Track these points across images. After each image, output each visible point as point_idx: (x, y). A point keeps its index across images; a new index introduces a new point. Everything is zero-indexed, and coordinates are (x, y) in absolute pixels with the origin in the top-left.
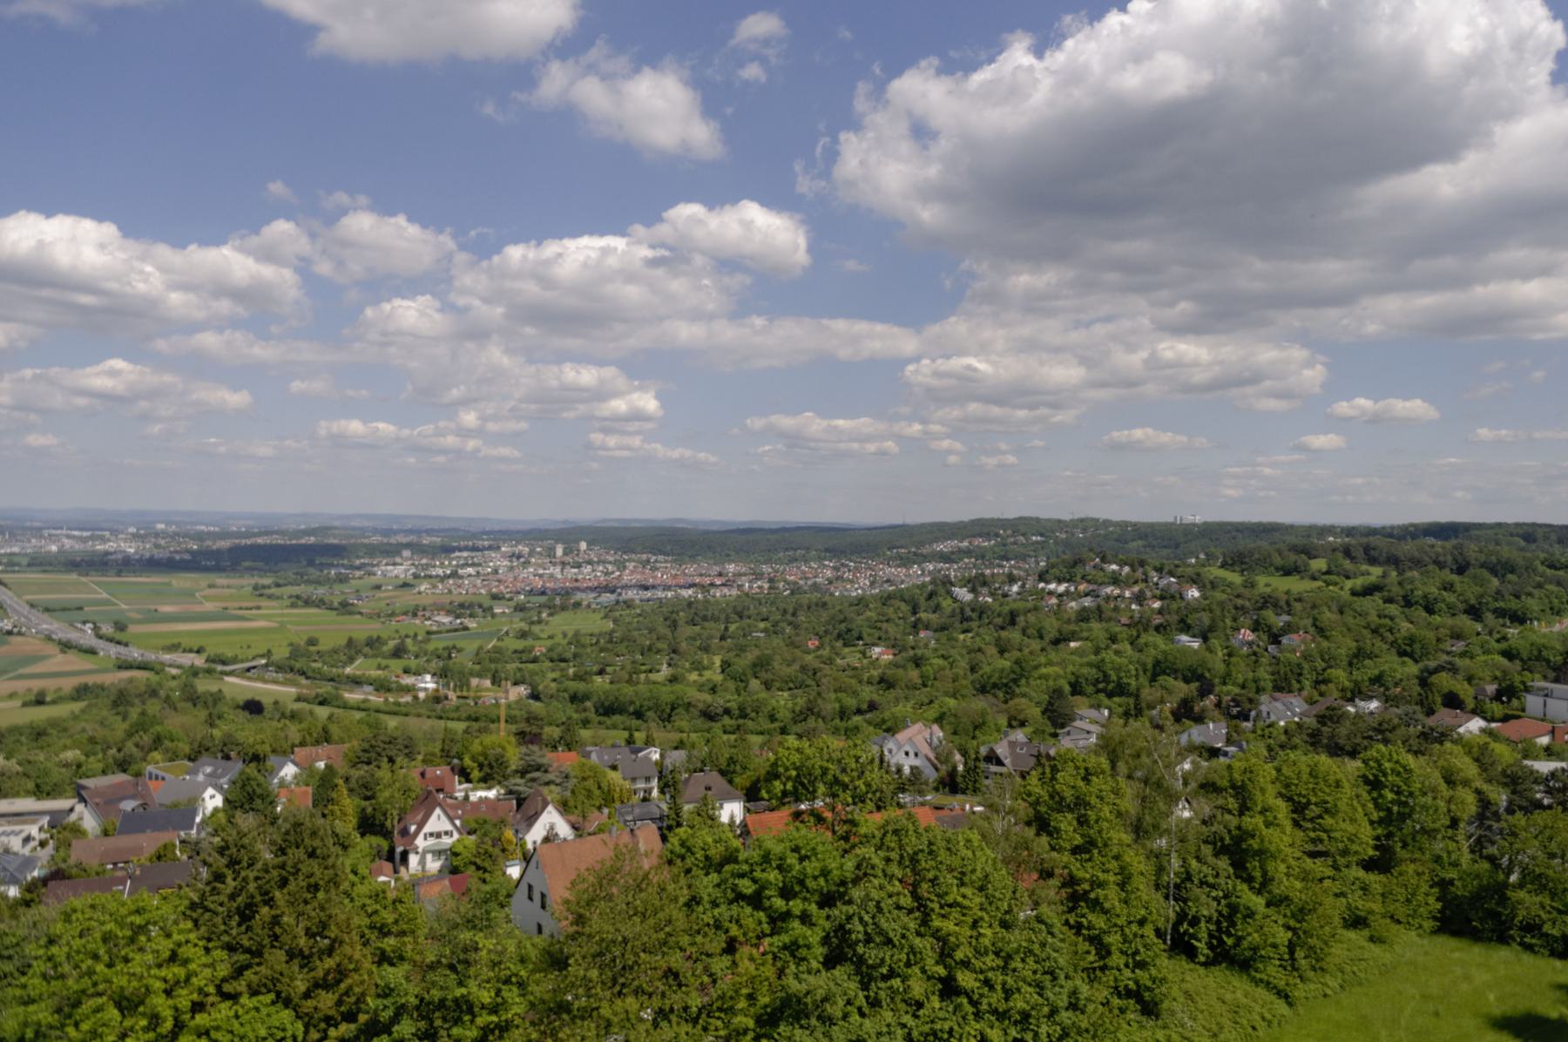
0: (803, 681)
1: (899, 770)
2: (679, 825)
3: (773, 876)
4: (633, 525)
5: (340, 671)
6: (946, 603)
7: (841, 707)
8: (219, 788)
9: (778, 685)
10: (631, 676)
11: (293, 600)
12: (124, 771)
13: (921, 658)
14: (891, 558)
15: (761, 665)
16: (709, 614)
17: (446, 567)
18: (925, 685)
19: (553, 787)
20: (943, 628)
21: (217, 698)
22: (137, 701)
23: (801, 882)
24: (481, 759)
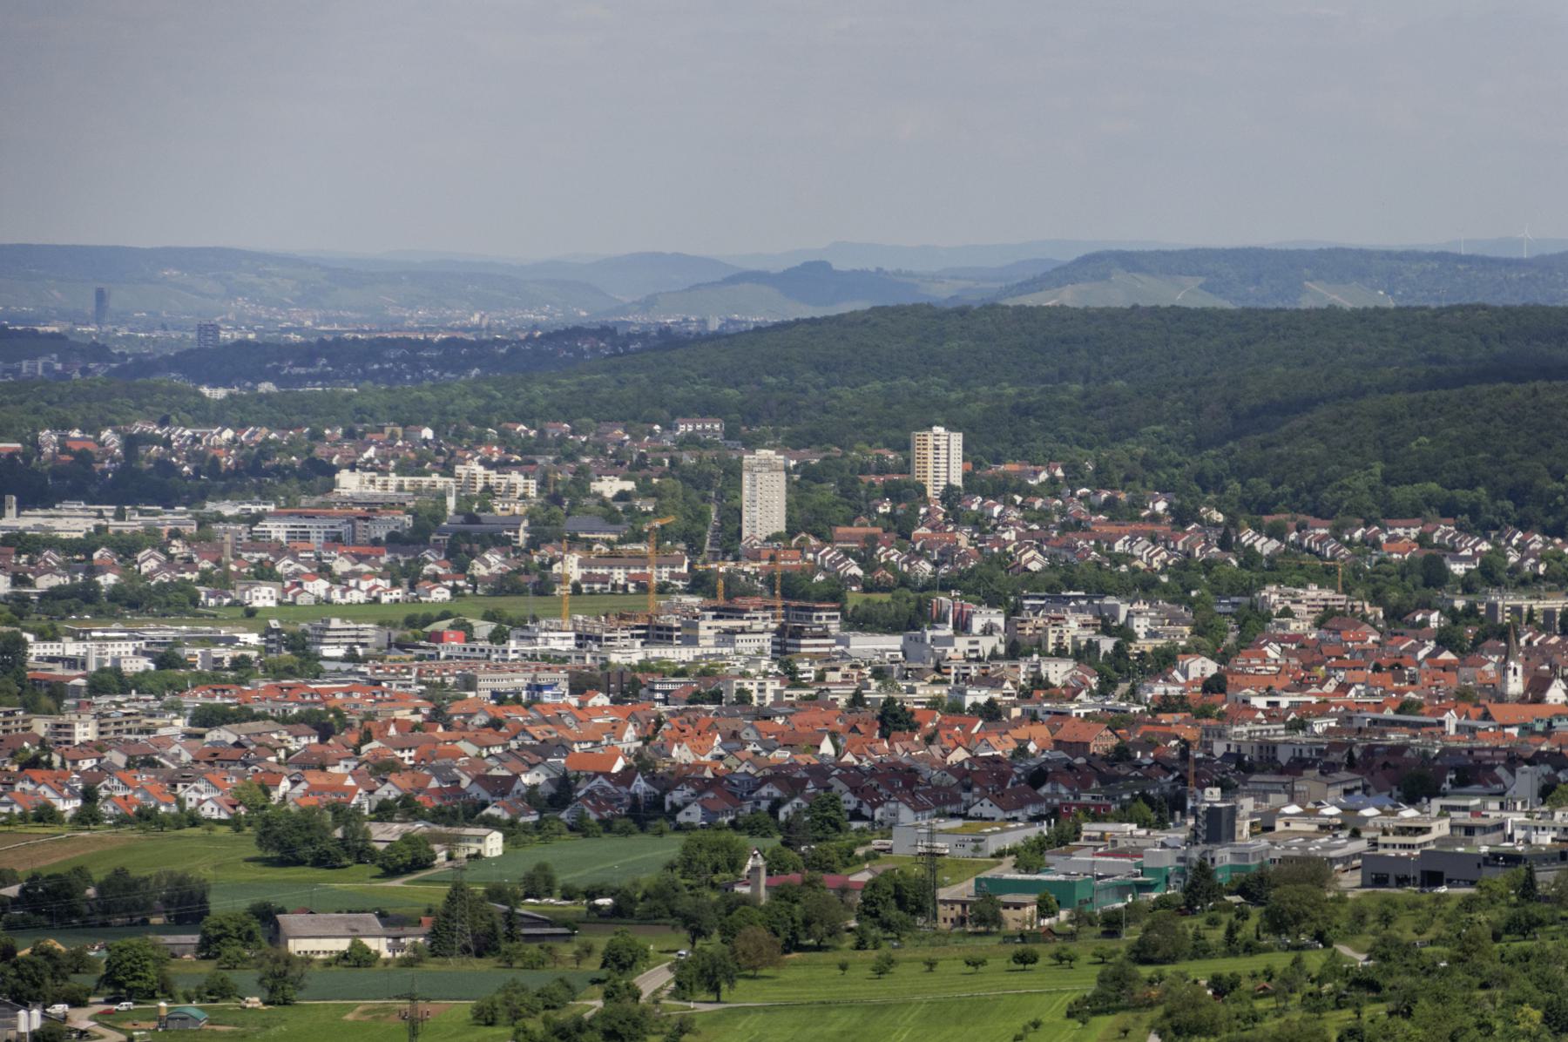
4: (1319, 295)
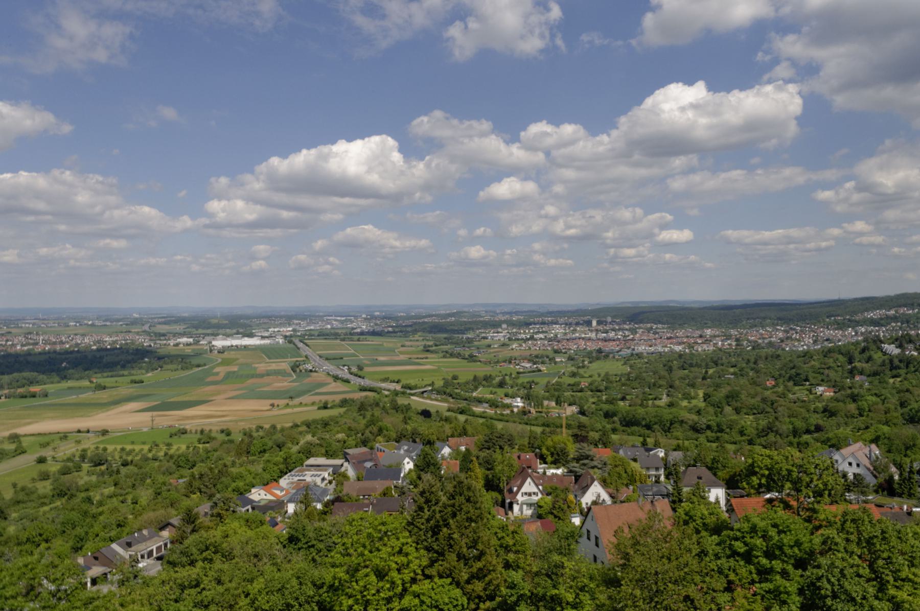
0: (764, 409)
1: (845, 476)
2: (681, 501)
3: (759, 542)
5: (470, 394)
6: (877, 356)
7: (794, 428)
8: (411, 459)
9: (745, 411)
10: (642, 402)
11: (444, 353)
12: (365, 446)
13: (857, 396)
14: (829, 324)
15: (731, 397)
16: (694, 362)
17: (527, 334)
18: (861, 415)
19: (596, 470)
20: (875, 374)
21: (408, 408)
22: (369, 408)
23: (780, 548)
24: (552, 450)
